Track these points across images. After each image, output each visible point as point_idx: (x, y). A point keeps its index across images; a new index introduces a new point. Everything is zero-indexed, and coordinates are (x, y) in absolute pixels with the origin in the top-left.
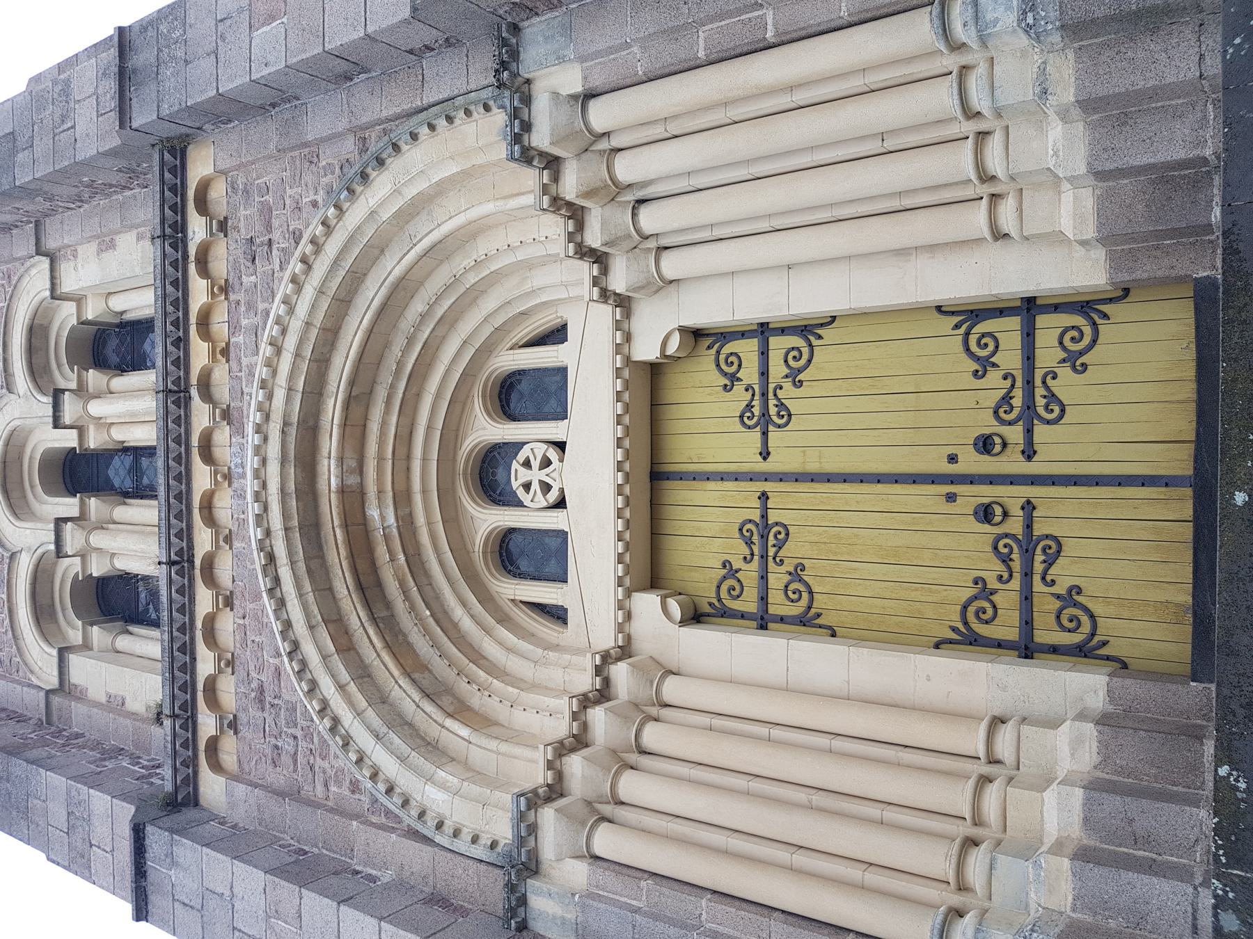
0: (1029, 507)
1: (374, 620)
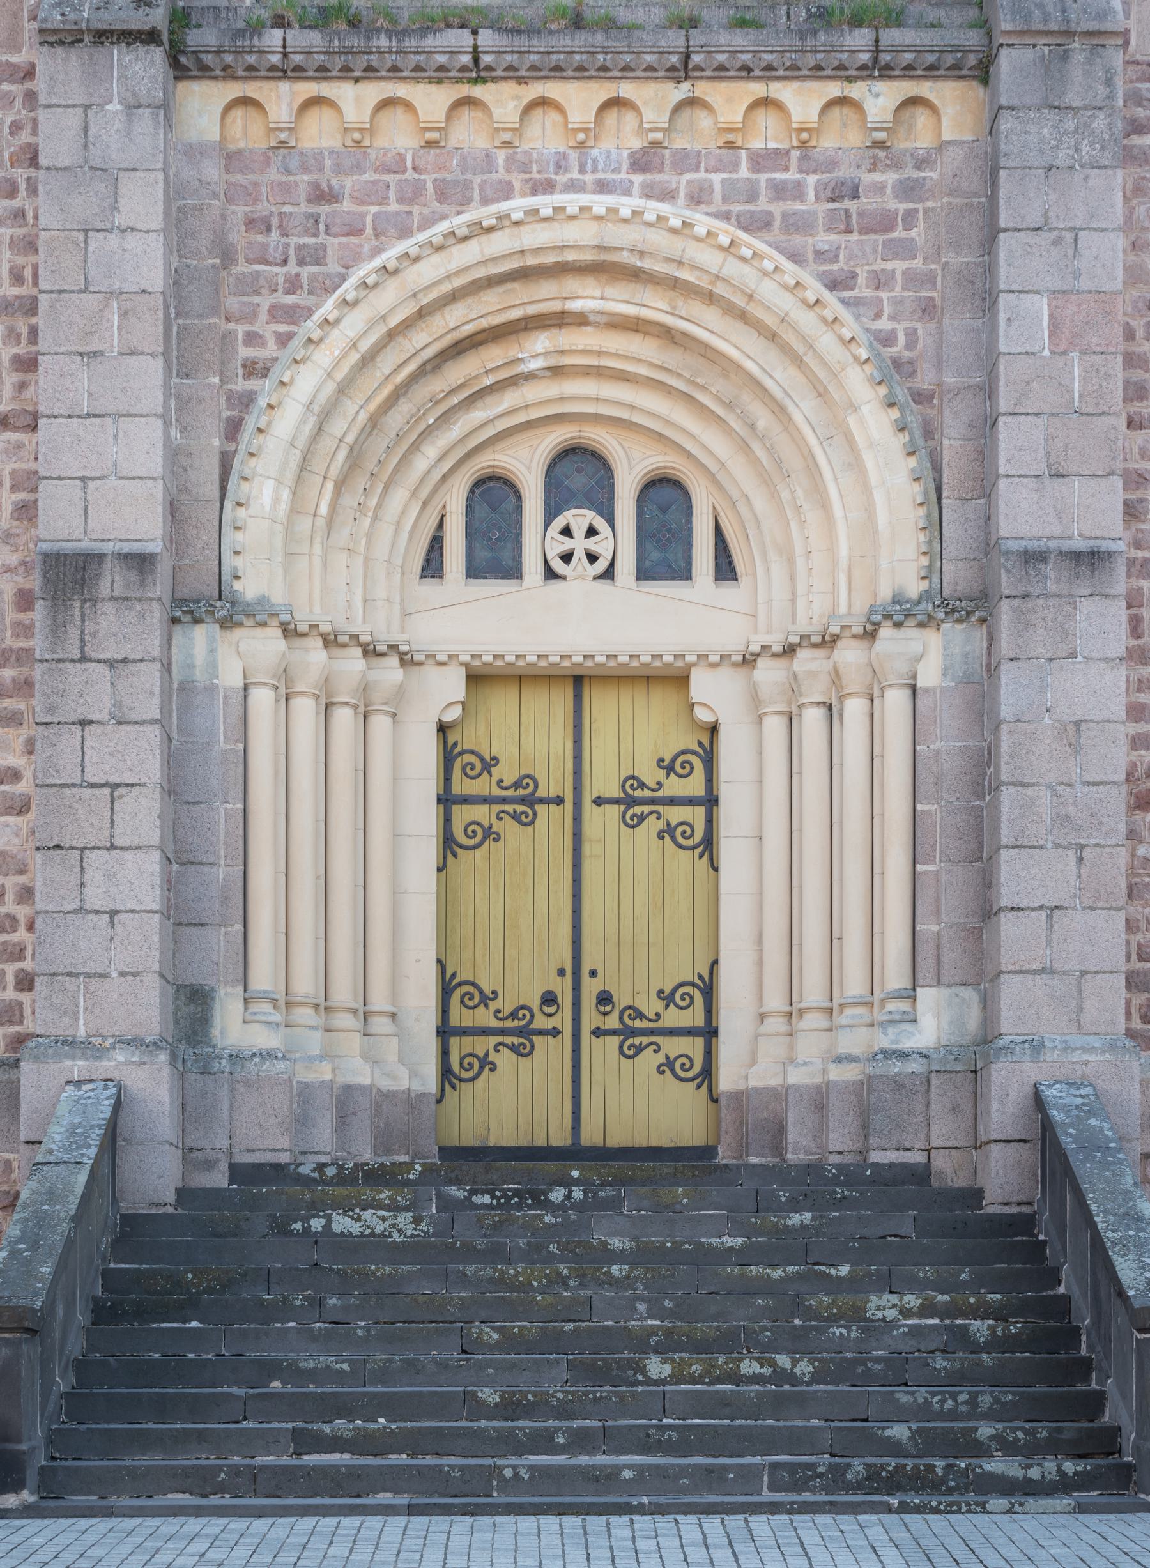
0: (555, 1032)
1: (424, 364)
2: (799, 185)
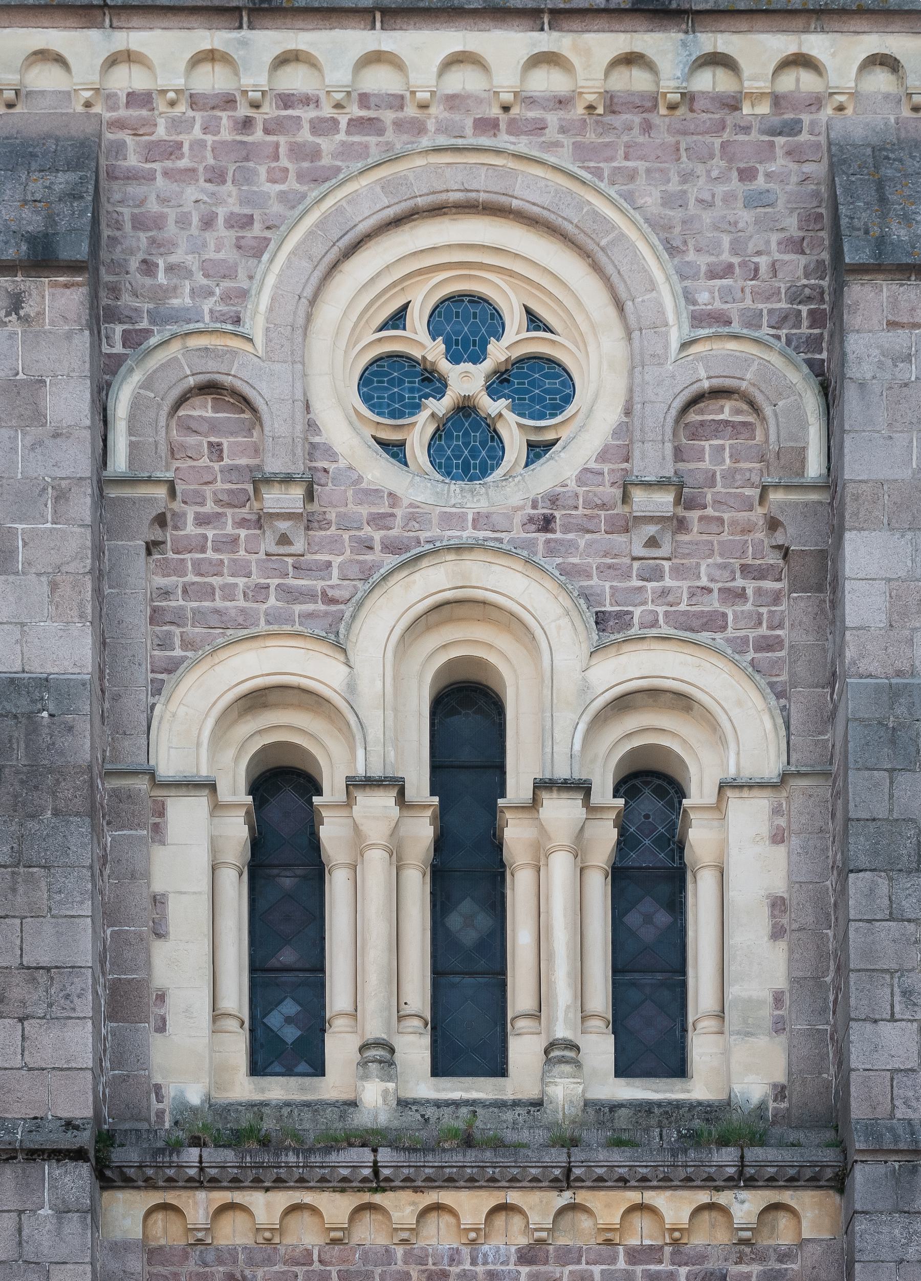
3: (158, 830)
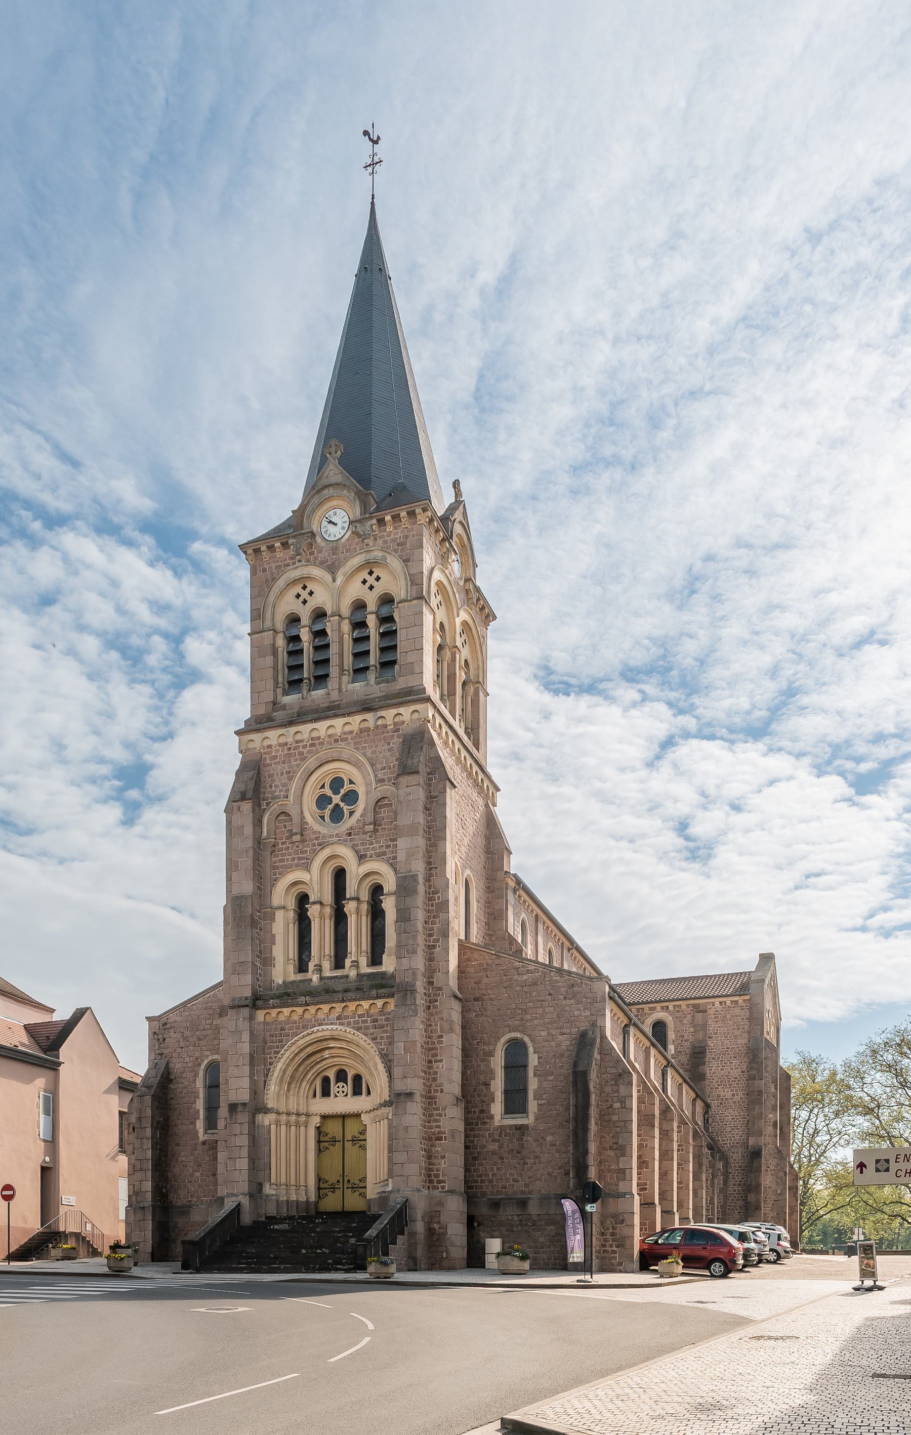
0: (339, 1188)
2: (367, 1020)
3: (274, 919)
